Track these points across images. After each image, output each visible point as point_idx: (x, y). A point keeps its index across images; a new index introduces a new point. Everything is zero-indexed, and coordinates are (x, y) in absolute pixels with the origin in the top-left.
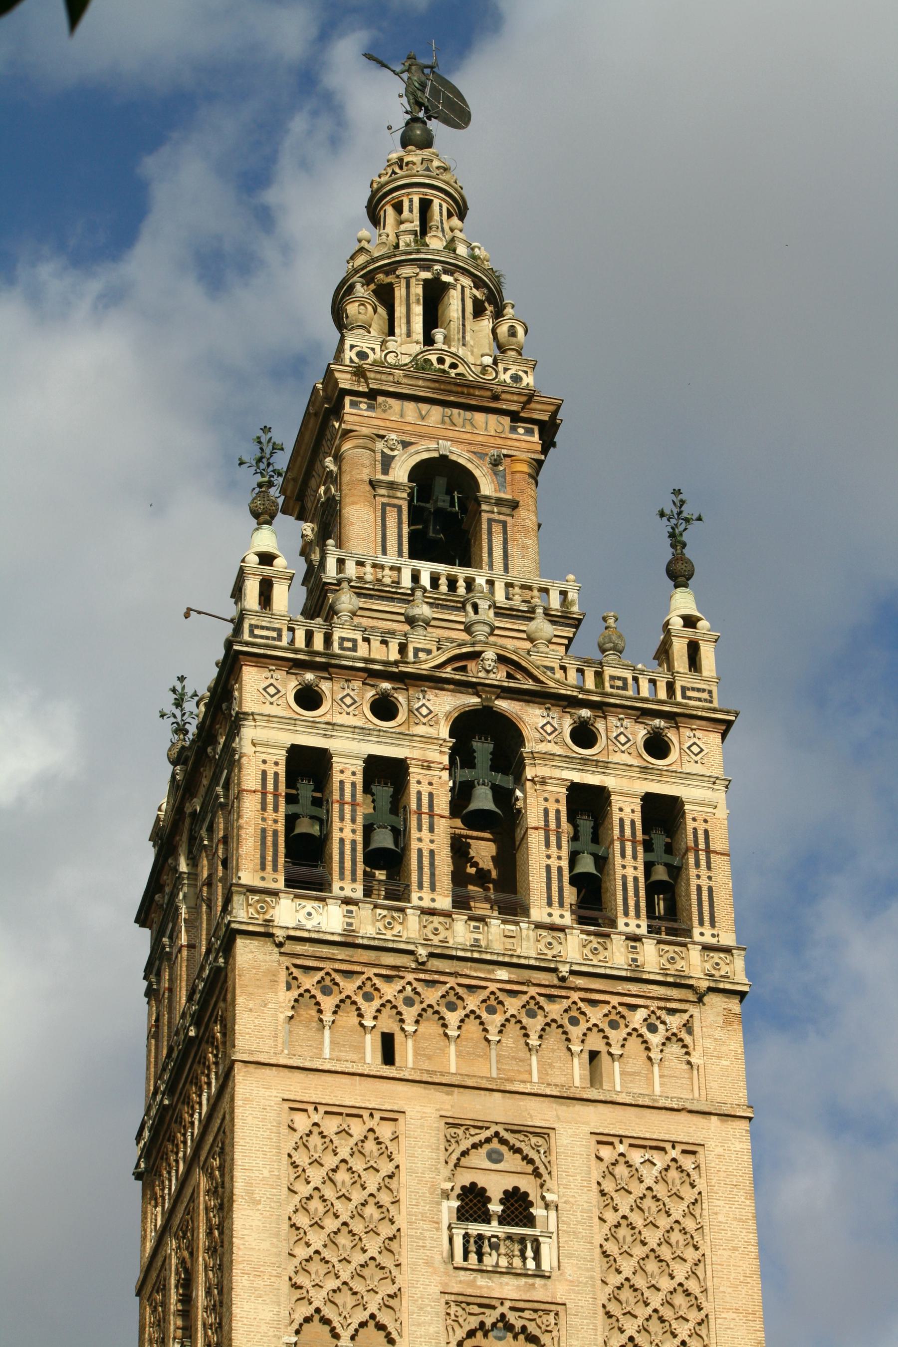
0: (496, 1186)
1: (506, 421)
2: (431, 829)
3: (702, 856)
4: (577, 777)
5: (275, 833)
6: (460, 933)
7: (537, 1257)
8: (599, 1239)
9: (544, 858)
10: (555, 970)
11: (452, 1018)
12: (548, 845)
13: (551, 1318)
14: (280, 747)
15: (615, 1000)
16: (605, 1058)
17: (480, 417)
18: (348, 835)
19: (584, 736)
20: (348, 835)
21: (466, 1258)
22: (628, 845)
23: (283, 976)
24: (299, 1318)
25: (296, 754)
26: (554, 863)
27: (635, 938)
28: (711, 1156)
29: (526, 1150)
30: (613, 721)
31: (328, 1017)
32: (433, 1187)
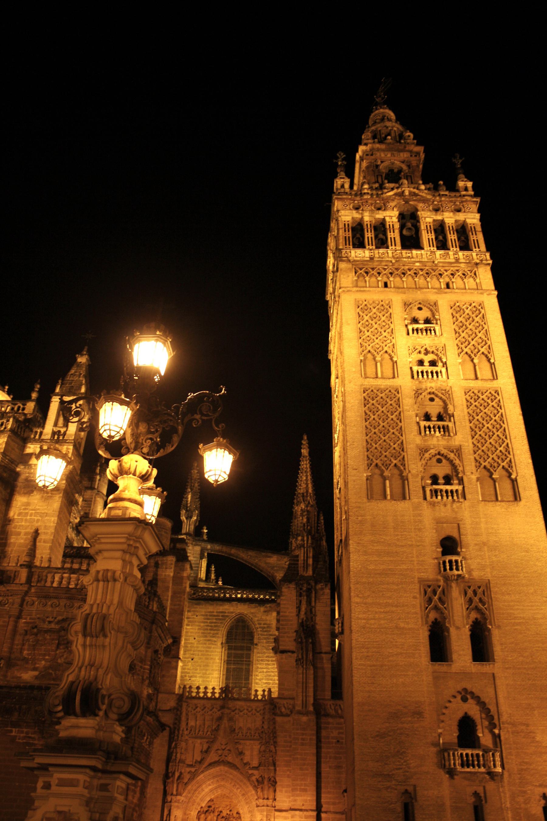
2: (394, 232)
3: (474, 233)
5: (349, 237)
7: (435, 332)
9: (426, 237)
10: (433, 262)
12: (428, 233)
15: (452, 268)
18: (370, 236)
20: (370, 236)
21: (413, 333)
22: (452, 232)
23: (354, 270)
26: (430, 237)
28: (485, 304)
31: (367, 279)
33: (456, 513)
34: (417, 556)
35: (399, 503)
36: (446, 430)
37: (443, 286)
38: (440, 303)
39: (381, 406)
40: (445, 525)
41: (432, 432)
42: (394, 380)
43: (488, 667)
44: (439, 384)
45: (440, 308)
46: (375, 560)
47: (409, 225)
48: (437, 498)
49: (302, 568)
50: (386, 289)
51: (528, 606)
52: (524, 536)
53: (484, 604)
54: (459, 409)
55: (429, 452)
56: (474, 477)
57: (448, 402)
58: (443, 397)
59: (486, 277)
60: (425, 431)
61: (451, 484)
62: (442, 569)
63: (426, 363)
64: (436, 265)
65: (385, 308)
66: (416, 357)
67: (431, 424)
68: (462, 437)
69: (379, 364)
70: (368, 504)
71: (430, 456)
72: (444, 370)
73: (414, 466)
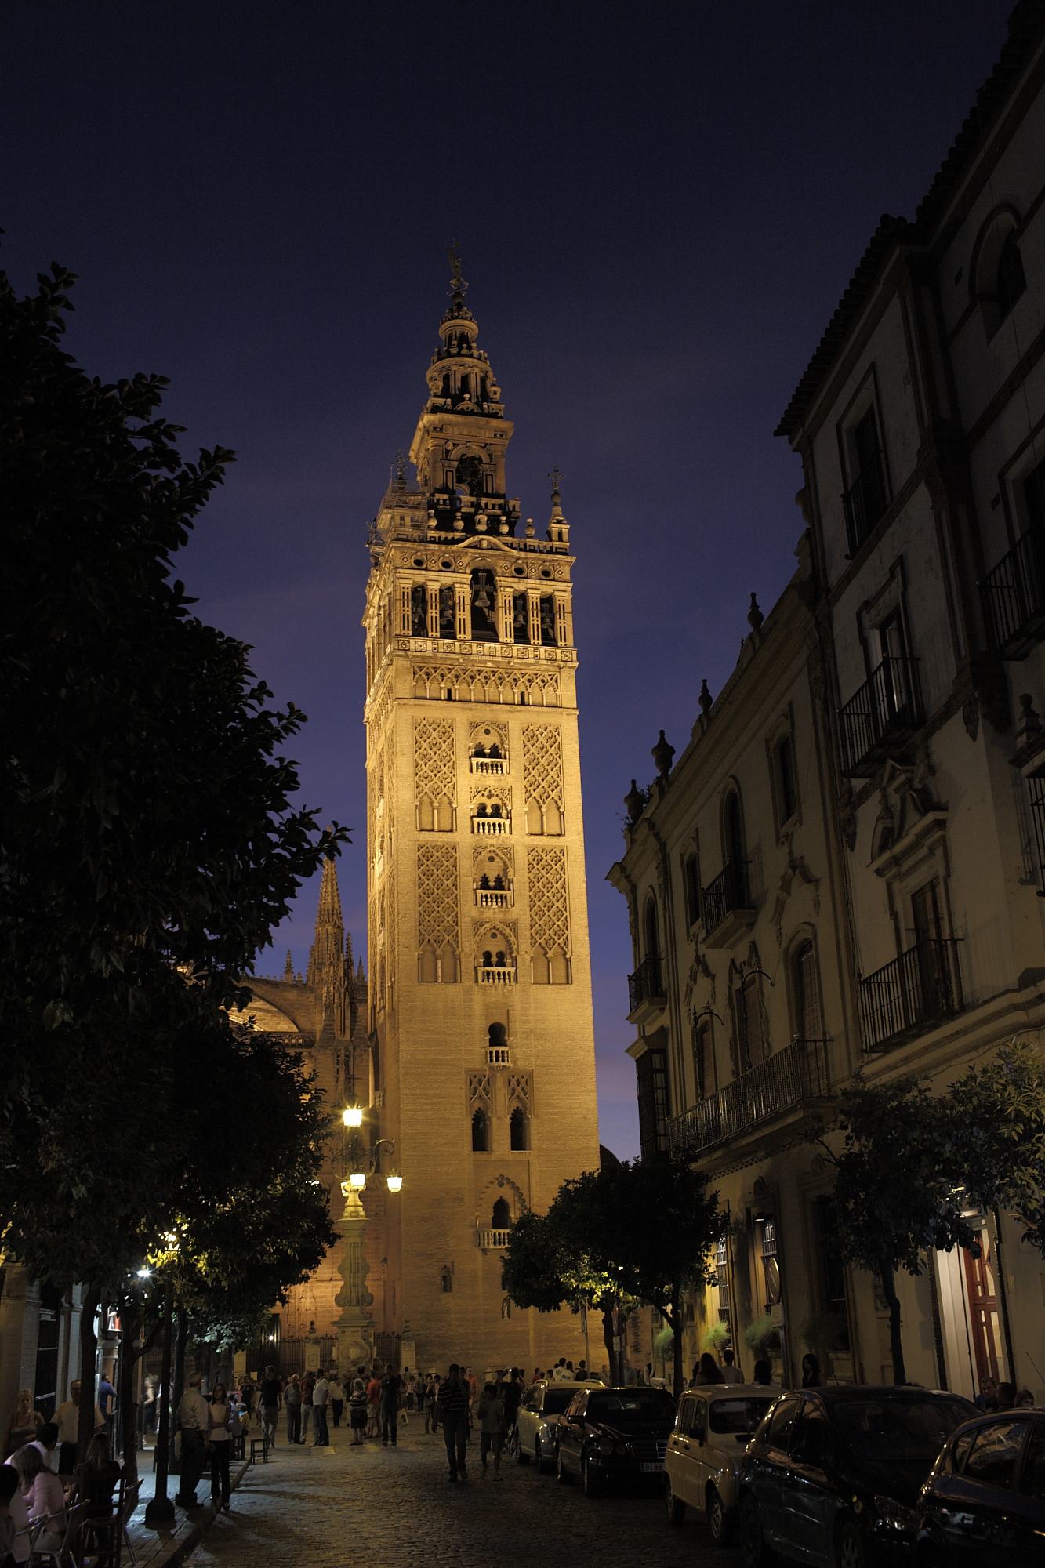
0: (488, 742)
9: (504, 619)
37: (517, 699)
38: (511, 726)
39: (433, 867)
47: (484, 594)
50: (450, 703)
54: (520, 875)
56: (528, 957)
59: (568, 691)
61: (504, 965)
63: (489, 811)
64: (512, 668)
65: (447, 731)
66: (479, 799)
67: (489, 892)
68: (520, 909)
72: (507, 823)
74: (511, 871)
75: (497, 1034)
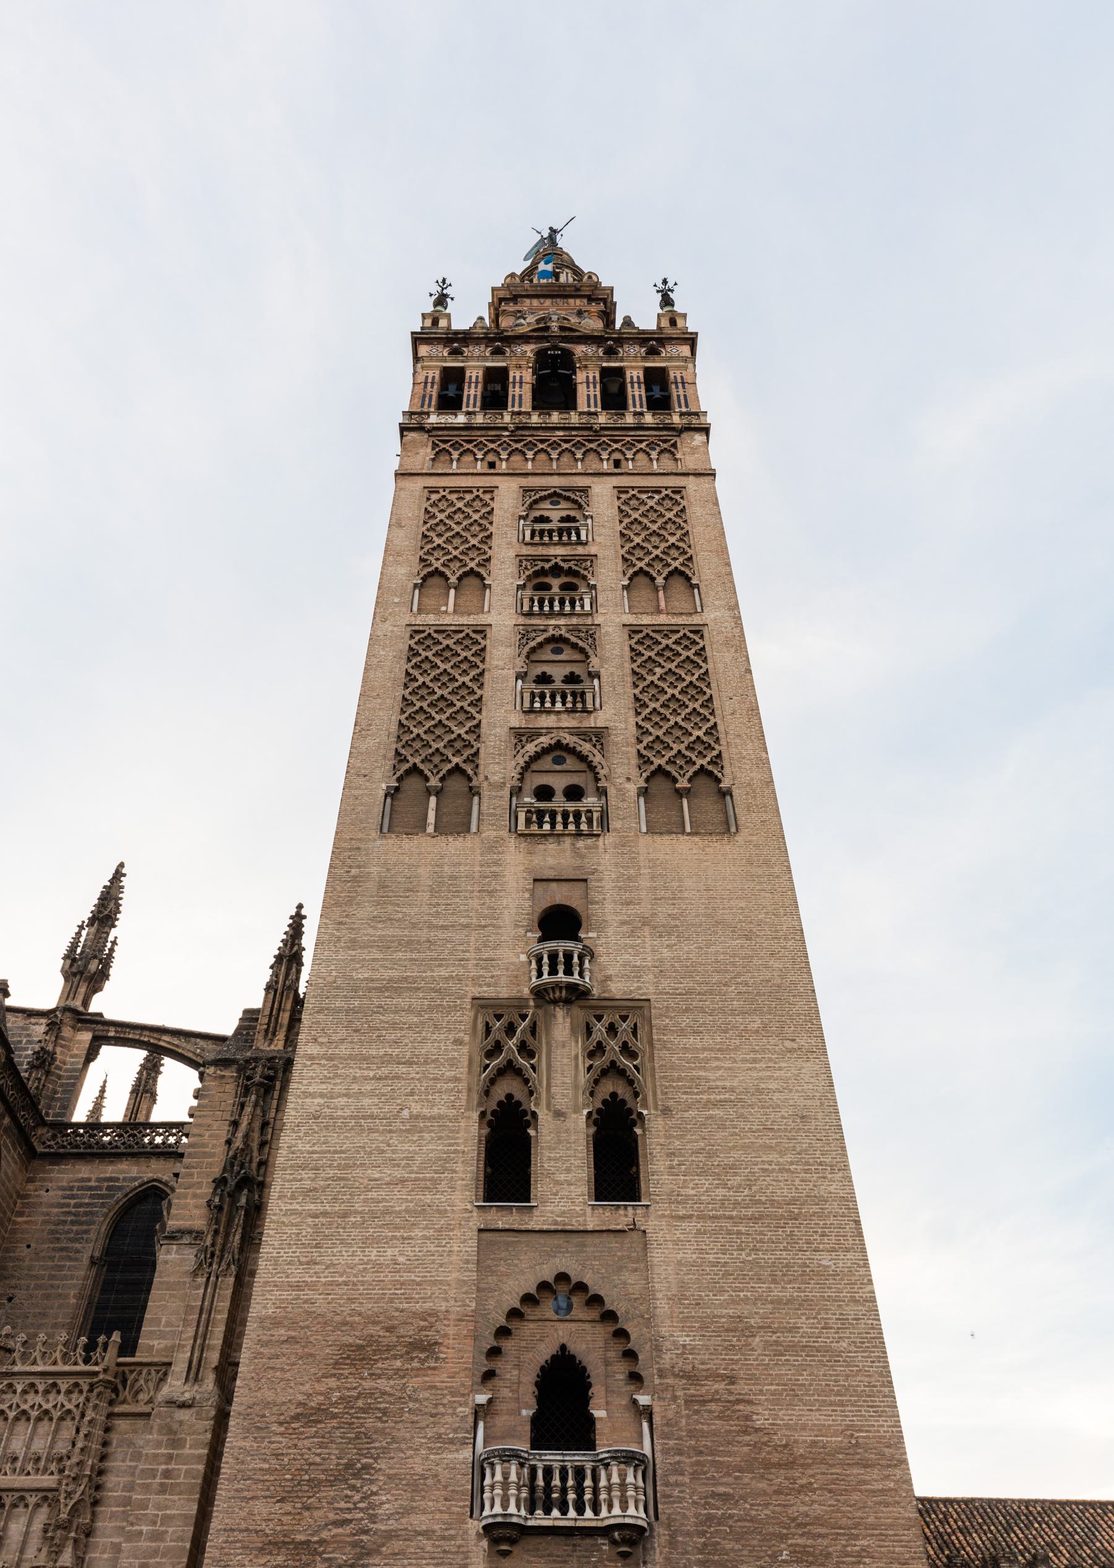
1: (585, 301)
2: (521, 387)
3: (680, 385)
4: (605, 364)
5: (431, 396)
6: (535, 419)
8: (619, 528)
11: (530, 455)
12: (588, 387)
13: (589, 563)
14: (437, 367)
16: (623, 463)
17: (571, 301)
19: (611, 352)
20: (472, 392)
21: (532, 537)
23: (430, 444)
24: (425, 572)
25: (445, 371)
26: (592, 394)
27: (641, 414)
29: (573, 496)
30: (626, 347)
32: (513, 515)
33: (582, 857)
34: (478, 949)
35: (451, 840)
36: (579, 699)
40: (554, 885)
41: (548, 705)
42: (481, 616)
43: (630, 1210)
44: (574, 621)
45: (595, 499)
46: (374, 960)
48: (541, 827)
49: (262, 1033)
51: (744, 1061)
52: (743, 905)
53: (633, 1055)
55: (536, 742)
56: (632, 788)
57: (591, 652)
58: (581, 643)
60: (532, 702)
62: (534, 973)
63: (556, 589)
69: (452, 592)
70: (379, 842)
71: (538, 749)
73: (497, 768)
74: (594, 661)
75: (559, 922)
